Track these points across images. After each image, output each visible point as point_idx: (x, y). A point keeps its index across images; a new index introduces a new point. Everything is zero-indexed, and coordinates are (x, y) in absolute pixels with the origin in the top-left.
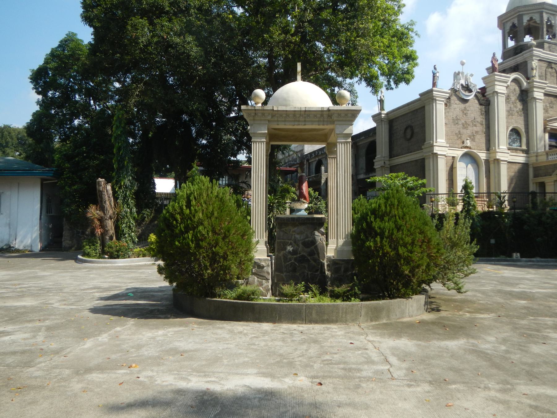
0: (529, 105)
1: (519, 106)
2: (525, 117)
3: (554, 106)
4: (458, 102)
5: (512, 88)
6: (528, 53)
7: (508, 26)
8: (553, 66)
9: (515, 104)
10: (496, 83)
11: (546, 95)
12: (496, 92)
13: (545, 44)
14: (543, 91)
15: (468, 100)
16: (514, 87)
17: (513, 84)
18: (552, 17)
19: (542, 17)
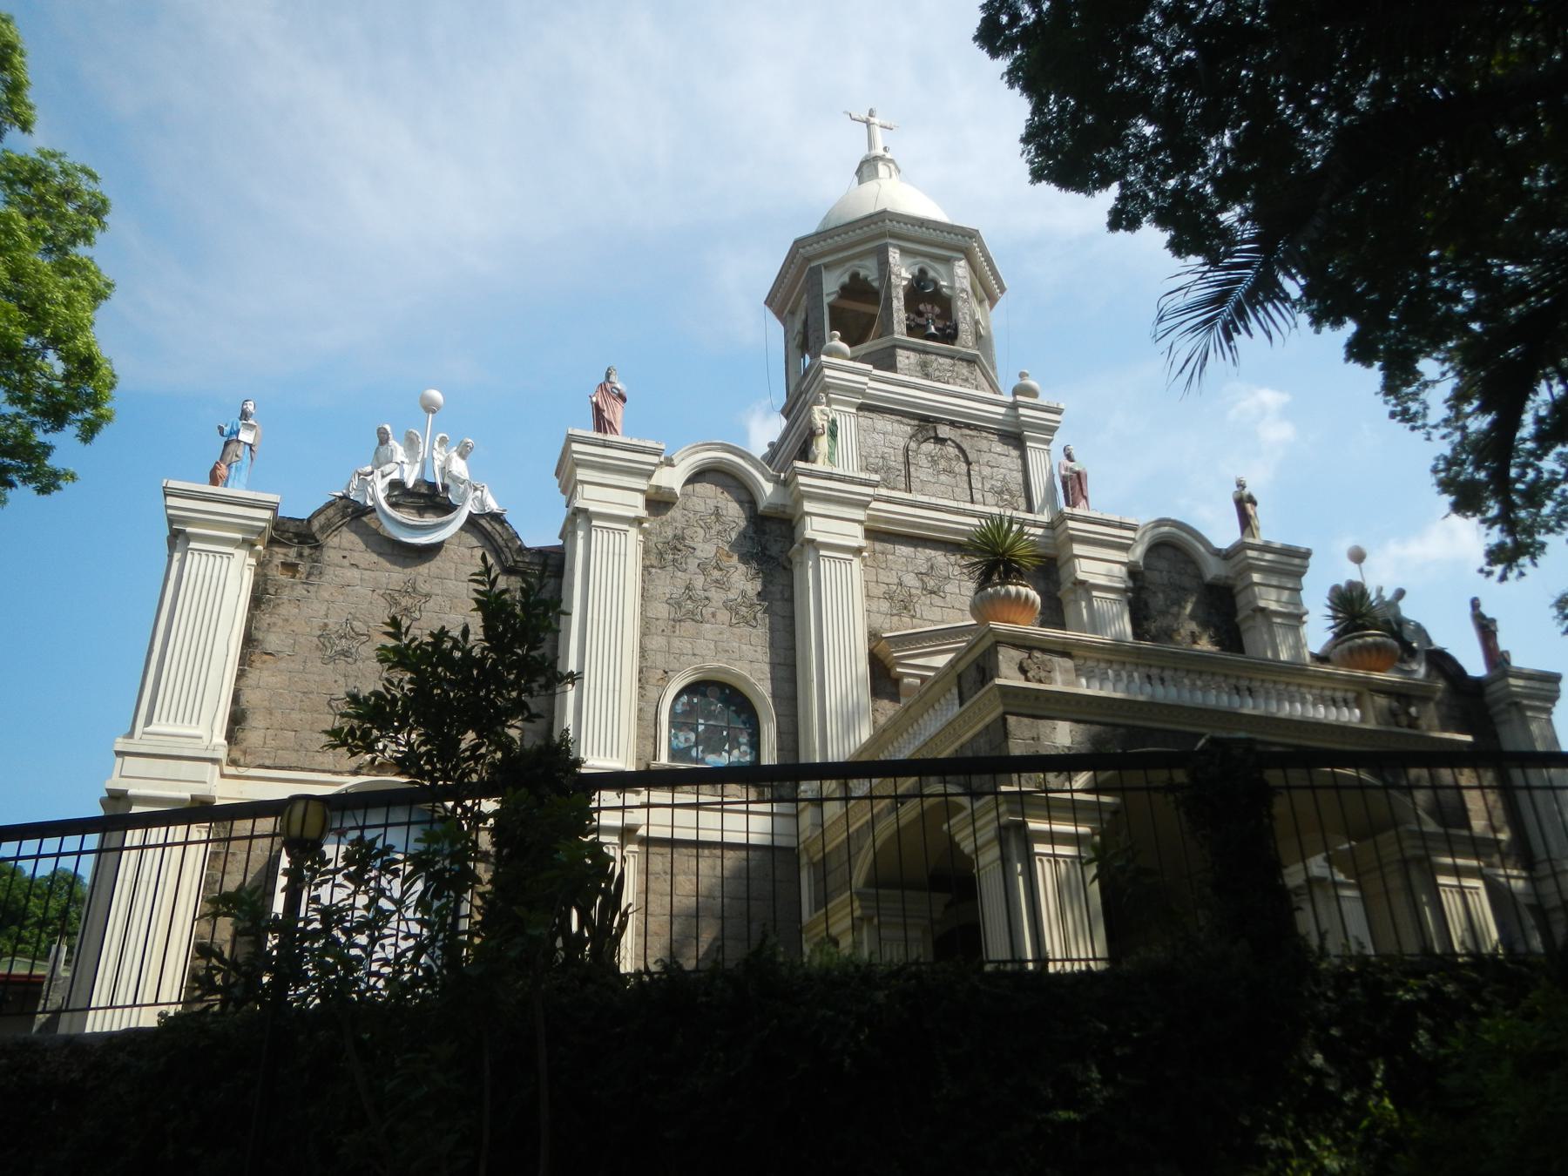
0: (797, 572)
1: (743, 581)
2: (772, 630)
3: (948, 588)
4: (375, 558)
5: (700, 507)
6: (816, 382)
7: (798, 326)
8: (944, 431)
9: (716, 574)
10: (582, 474)
11: (872, 534)
12: (585, 511)
13: (899, 352)
14: (860, 514)
15: (432, 550)
16: (711, 503)
17: (708, 492)
18: (940, 267)
19: (884, 264)
